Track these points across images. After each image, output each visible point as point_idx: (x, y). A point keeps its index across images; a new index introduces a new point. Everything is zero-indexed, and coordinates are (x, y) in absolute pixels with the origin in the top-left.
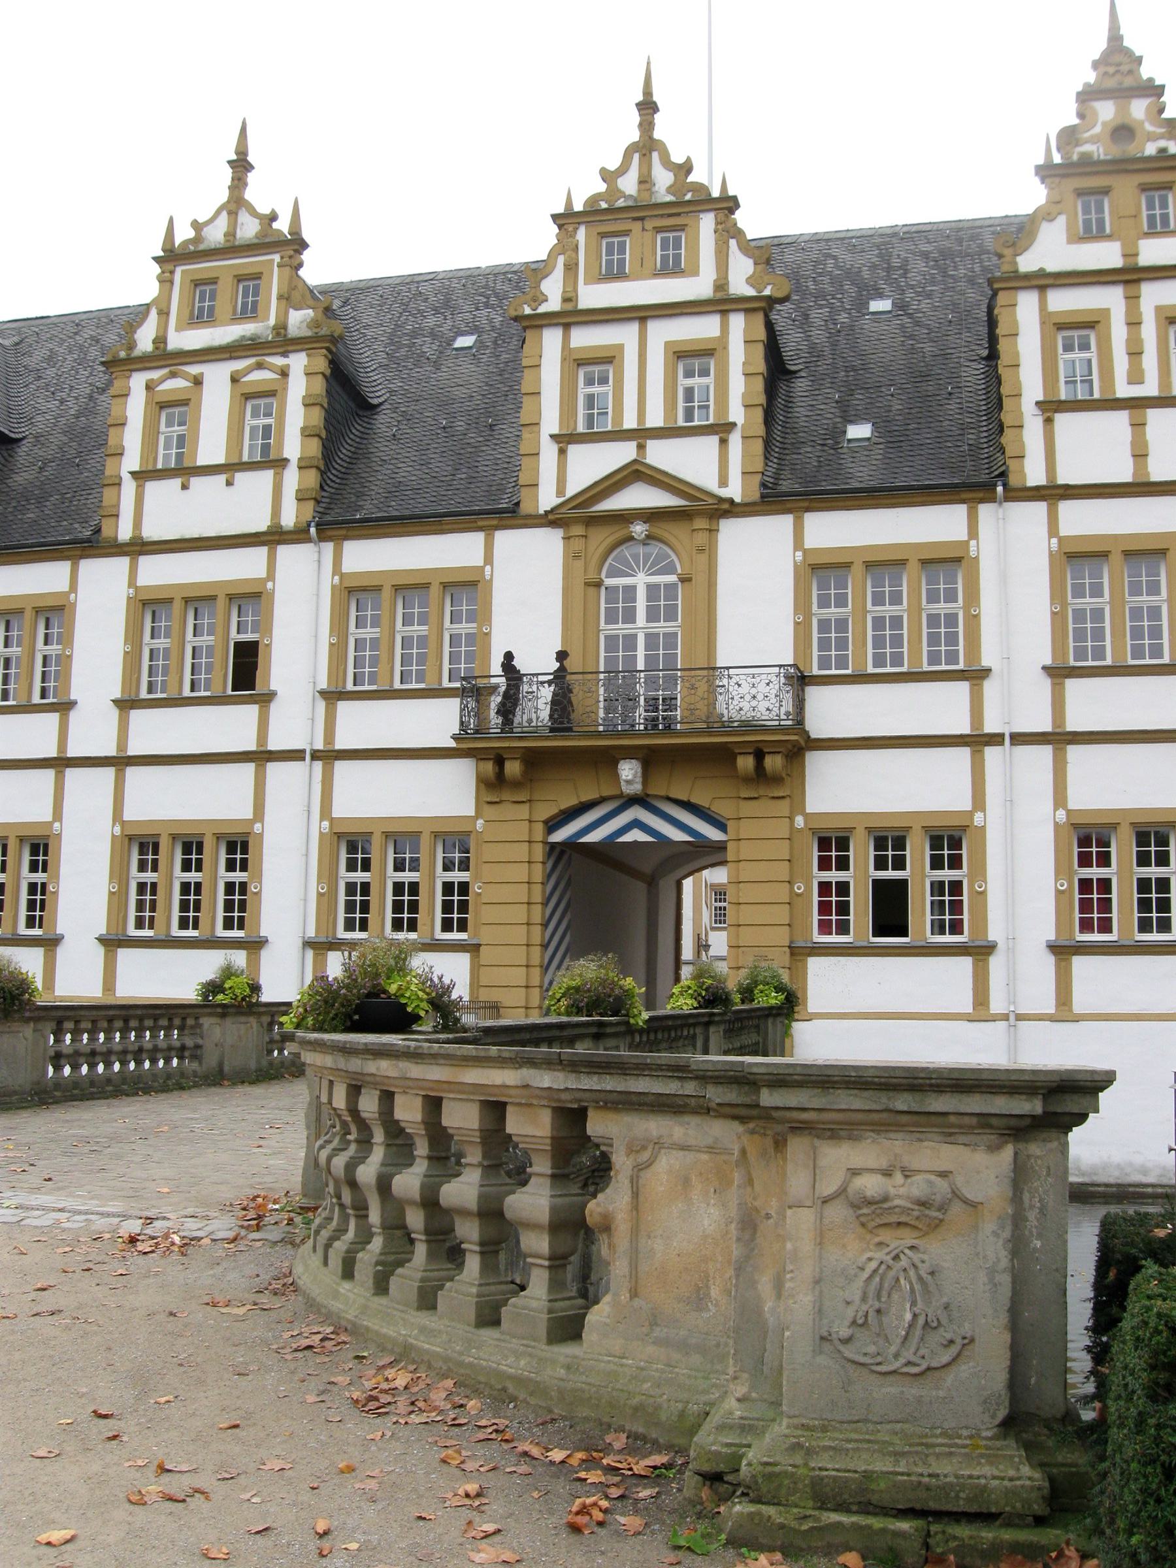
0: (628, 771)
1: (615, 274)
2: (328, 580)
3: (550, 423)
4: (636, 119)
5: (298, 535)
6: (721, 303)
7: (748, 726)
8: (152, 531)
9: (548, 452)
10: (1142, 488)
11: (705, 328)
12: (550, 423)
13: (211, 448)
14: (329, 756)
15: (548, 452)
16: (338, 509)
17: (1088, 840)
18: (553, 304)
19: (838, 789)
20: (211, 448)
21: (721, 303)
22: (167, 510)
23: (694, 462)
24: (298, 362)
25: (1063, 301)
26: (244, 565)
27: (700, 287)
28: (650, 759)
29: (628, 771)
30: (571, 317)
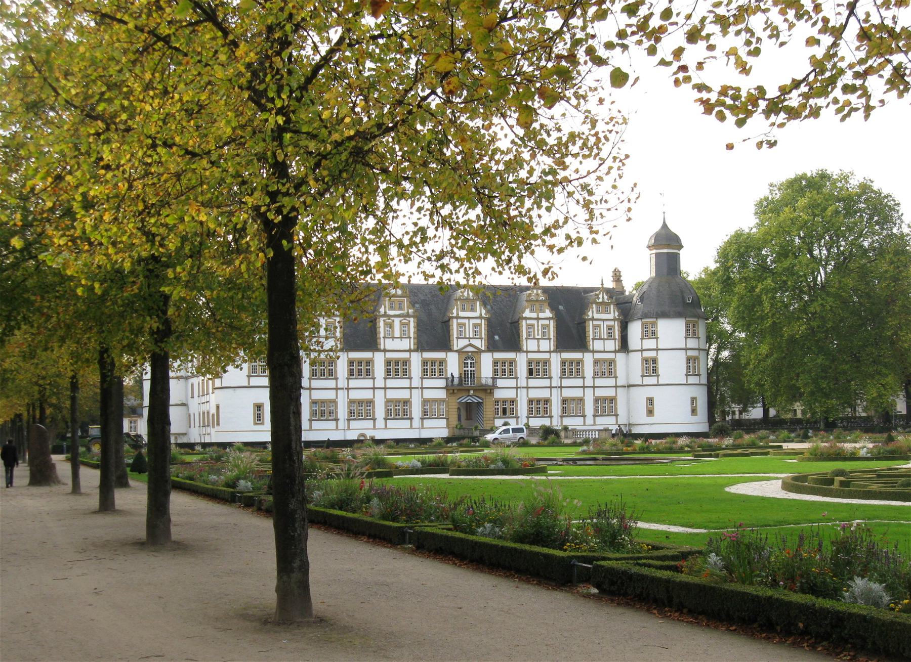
0: (472, 392)
1: (463, 310)
2: (420, 359)
3: (455, 336)
5: (414, 351)
6: (481, 317)
7: (486, 385)
8: (387, 348)
9: (455, 340)
10: (539, 352)
11: (478, 321)
12: (455, 336)
13: (397, 334)
14: (422, 388)
15: (455, 340)
16: (421, 346)
17: (530, 401)
18: (455, 315)
19: (499, 394)
20: (397, 334)
21: (481, 317)
22: (389, 344)
23: (477, 343)
24: (412, 320)
25: (529, 322)
26: (406, 355)
27: (477, 314)
28: (474, 390)
29: (472, 392)
30: (458, 317)
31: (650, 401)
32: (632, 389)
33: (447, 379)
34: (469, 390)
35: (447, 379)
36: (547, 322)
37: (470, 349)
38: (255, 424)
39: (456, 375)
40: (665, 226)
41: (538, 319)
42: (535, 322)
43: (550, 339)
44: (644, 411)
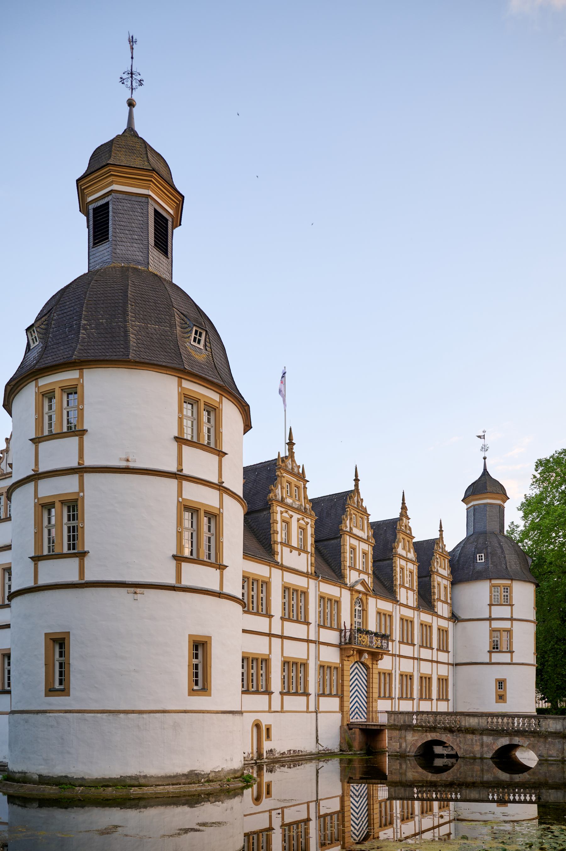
4: (354, 483)
6: (366, 541)
9: (348, 569)
10: (407, 606)
18: (348, 529)
31: (501, 684)
32: (459, 667)
33: (341, 631)
34: (360, 653)
35: (341, 631)
36: (410, 566)
37: (359, 587)
38: (192, 692)
39: (348, 627)
40: (485, 473)
41: (407, 560)
42: (403, 563)
43: (414, 591)
44: (493, 696)
